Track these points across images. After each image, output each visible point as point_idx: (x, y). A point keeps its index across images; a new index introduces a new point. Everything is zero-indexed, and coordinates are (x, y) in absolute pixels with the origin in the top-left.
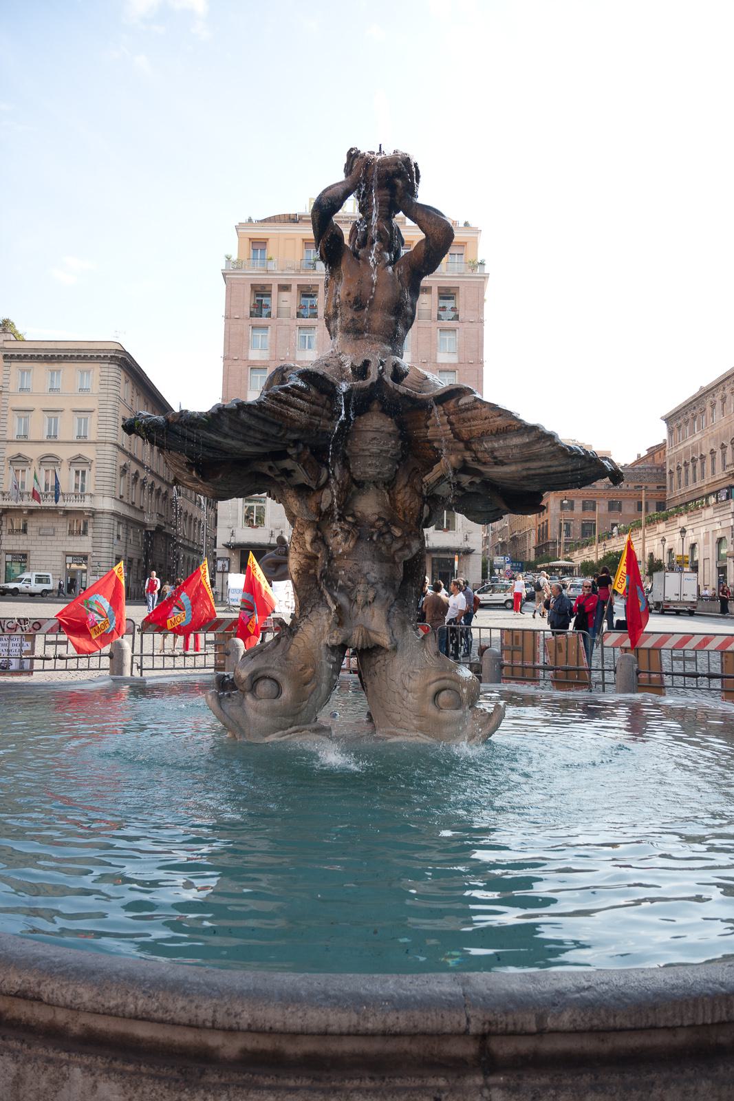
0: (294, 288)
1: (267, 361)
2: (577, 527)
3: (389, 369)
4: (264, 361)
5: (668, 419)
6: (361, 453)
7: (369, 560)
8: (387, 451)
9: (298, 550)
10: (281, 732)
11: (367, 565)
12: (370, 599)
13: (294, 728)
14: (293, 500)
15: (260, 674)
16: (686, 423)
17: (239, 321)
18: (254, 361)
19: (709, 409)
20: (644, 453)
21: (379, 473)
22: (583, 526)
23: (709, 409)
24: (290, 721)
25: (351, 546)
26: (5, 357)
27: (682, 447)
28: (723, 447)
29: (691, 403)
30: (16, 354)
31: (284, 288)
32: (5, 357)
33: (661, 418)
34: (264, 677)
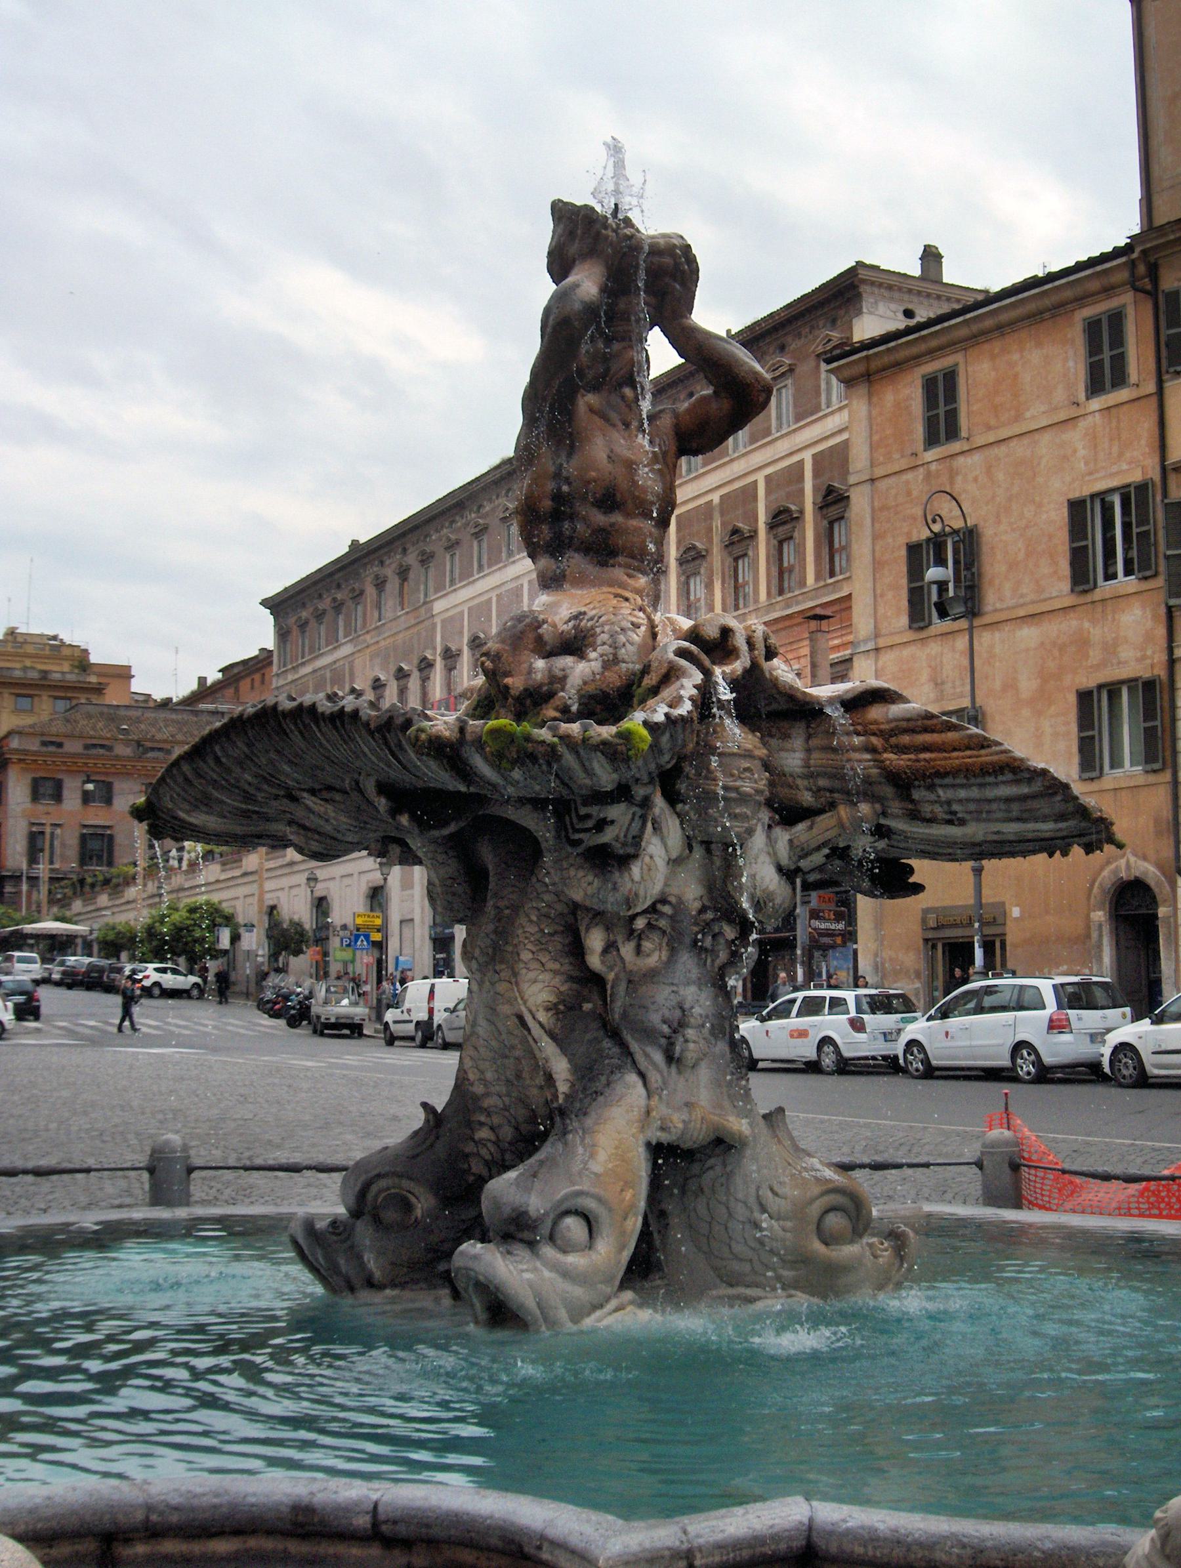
2: (67, 844)
5: (277, 605)
7: (694, 983)
9: (552, 965)
10: (598, 1313)
11: (690, 993)
14: (581, 873)
15: (564, 1207)
16: (320, 616)
19: (370, 591)
20: (213, 676)
22: (83, 838)
23: (370, 591)
25: (664, 958)
27: (307, 669)
28: (401, 675)
29: (331, 574)
33: (265, 603)
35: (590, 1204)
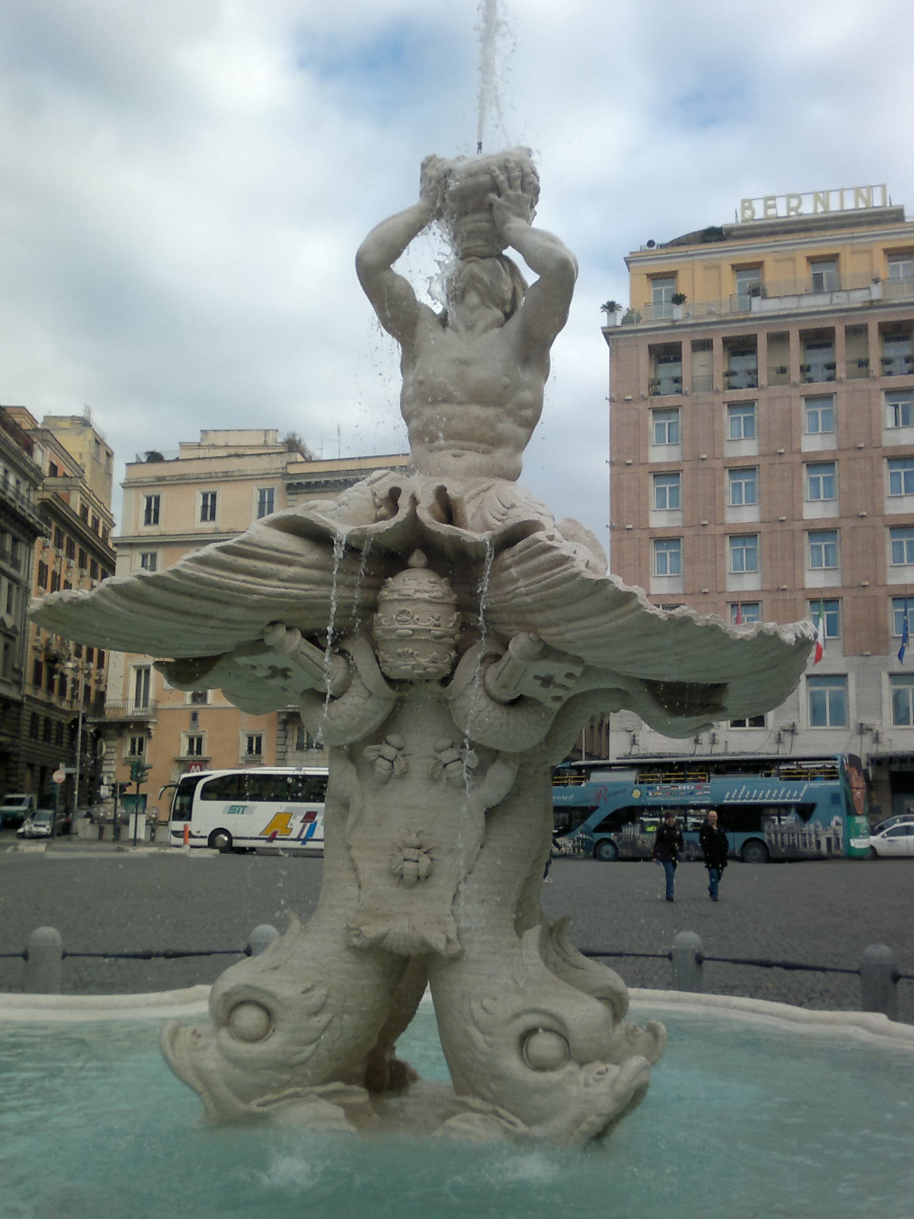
0: (718, 344)
1: (679, 463)
3: (427, 501)
4: (674, 463)
6: (387, 637)
8: (430, 631)
12: (423, 872)
13: (291, 1091)
17: (633, 405)
18: (659, 464)
21: (413, 668)
24: (286, 1077)
26: (289, 487)
30: (304, 481)
31: (704, 346)
32: (289, 487)
34: (242, 1003)
35: (265, 1000)
